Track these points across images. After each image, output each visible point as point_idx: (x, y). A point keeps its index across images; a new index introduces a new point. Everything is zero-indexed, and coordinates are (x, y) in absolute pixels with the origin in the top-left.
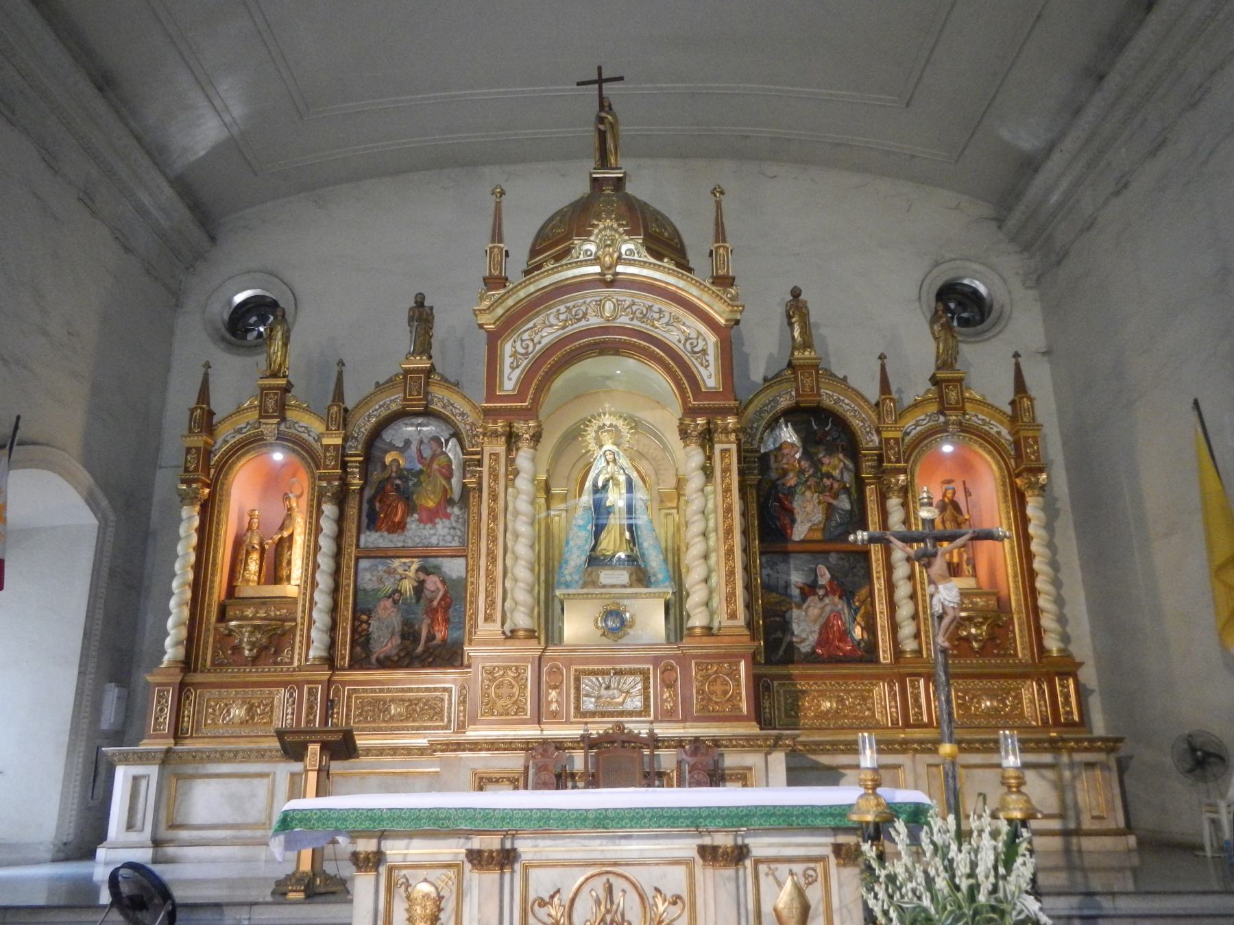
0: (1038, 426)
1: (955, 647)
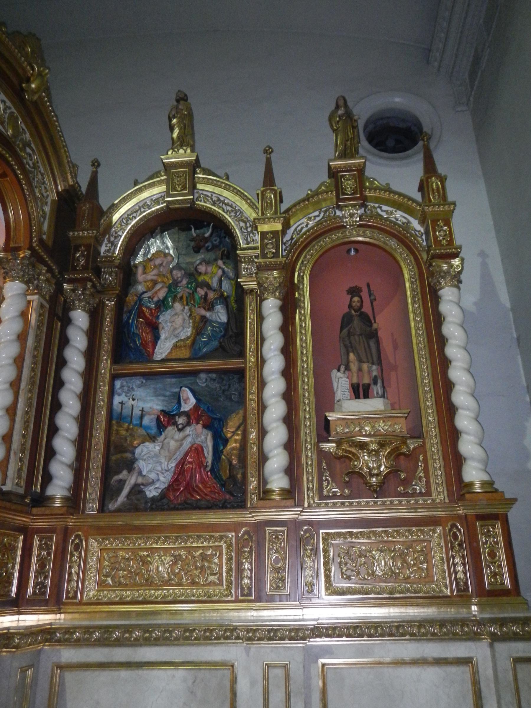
0: (449, 204)
1: (347, 484)
